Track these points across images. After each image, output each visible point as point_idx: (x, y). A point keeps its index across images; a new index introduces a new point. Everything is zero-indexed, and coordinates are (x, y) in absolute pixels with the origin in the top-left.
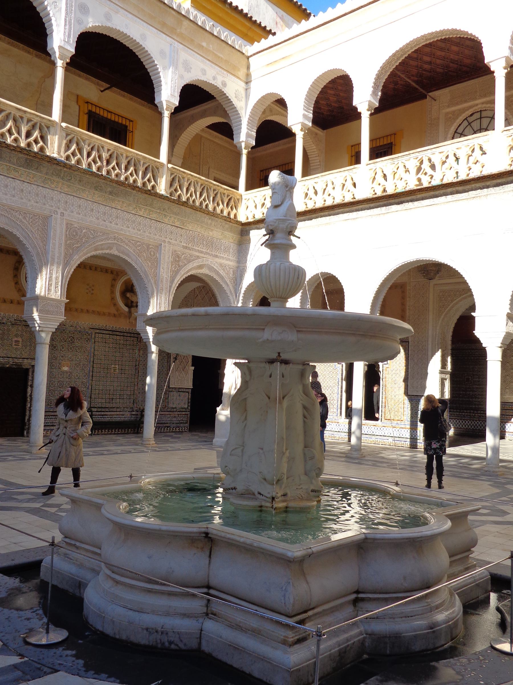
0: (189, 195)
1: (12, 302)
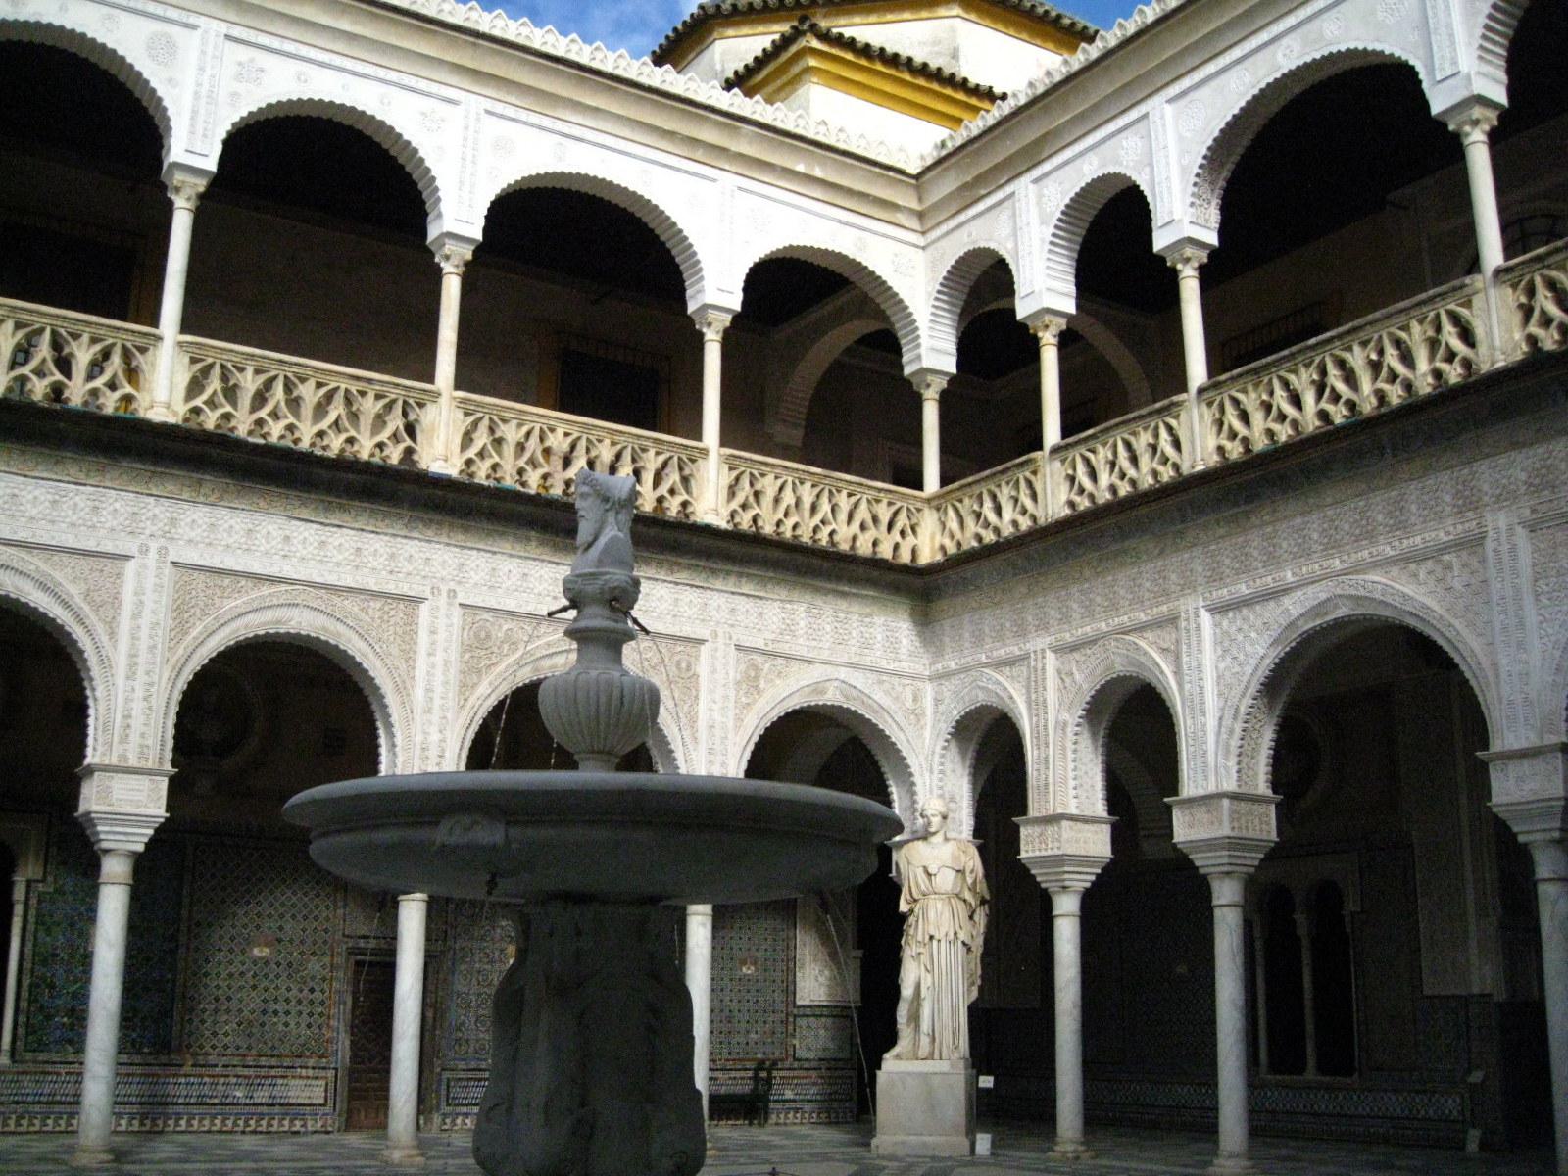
0: (780, 515)
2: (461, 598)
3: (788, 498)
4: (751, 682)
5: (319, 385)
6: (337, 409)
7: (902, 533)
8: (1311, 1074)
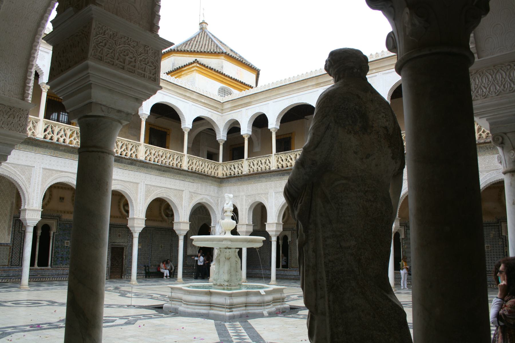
1: (117, 217)
2: (146, 183)
3: (198, 164)
4: (191, 198)
6: (124, 147)
8: (281, 268)
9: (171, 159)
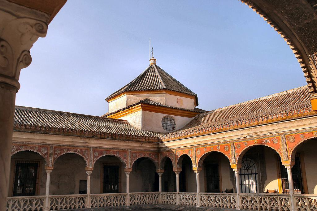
3: (139, 198)
5: (70, 198)
6: (73, 202)
7: (156, 199)
9: (116, 200)
